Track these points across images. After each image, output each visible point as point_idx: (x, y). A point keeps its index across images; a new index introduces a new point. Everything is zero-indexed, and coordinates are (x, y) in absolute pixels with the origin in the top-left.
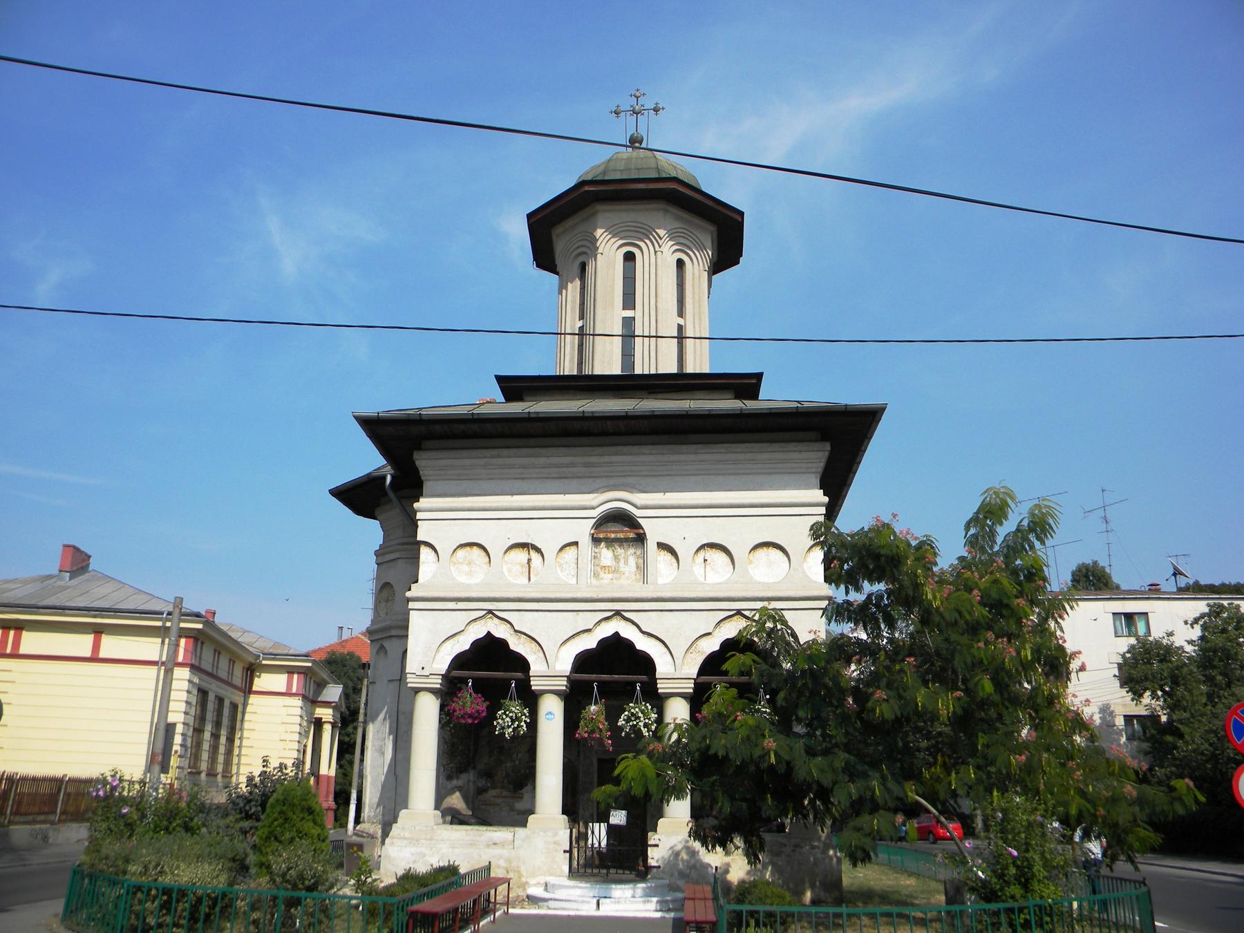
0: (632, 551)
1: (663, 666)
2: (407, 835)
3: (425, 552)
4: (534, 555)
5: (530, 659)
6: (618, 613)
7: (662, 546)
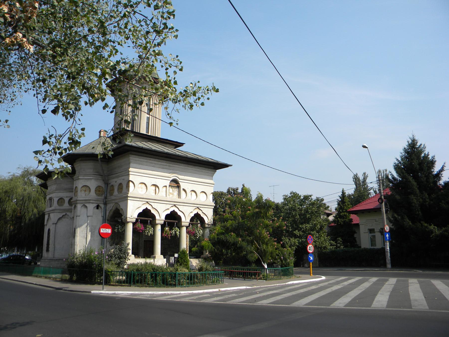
6: (175, 205)
7: (184, 190)
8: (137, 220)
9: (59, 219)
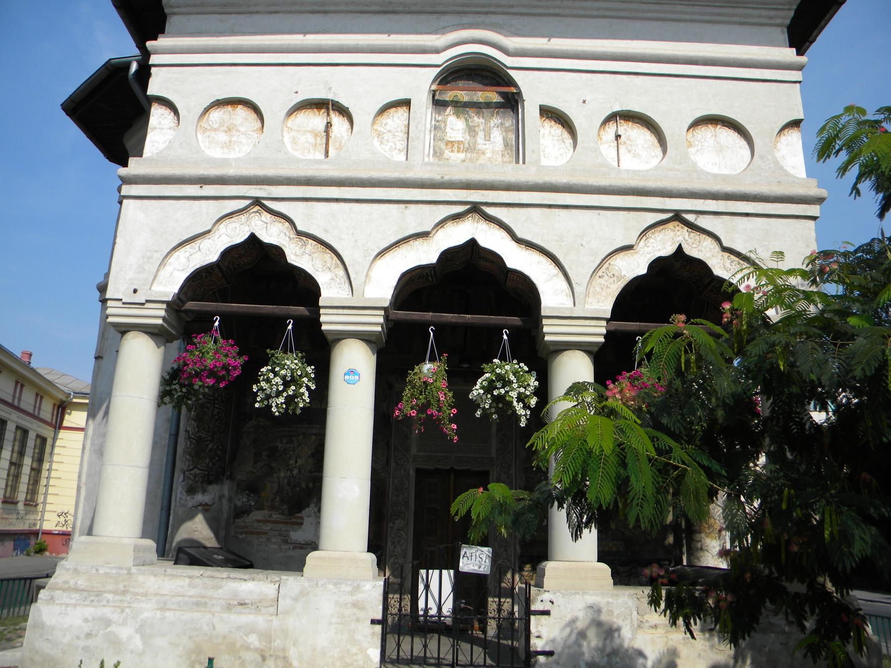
0: (496, 121)
1: (553, 297)
2: (82, 582)
3: (158, 116)
4: (337, 120)
5: (321, 278)
6: (475, 209)
7: (549, 113)
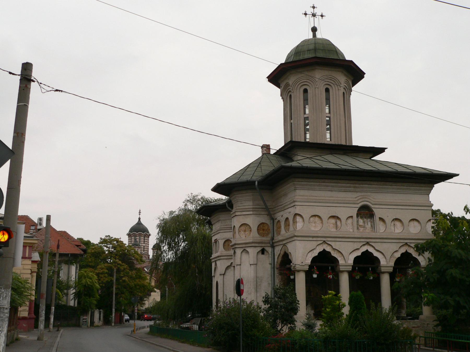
0: (369, 220)
1: (383, 262)
5: (339, 259)
6: (368, 243)
7: (381, 219)
8: (311, 267)
9: (228, 268)
